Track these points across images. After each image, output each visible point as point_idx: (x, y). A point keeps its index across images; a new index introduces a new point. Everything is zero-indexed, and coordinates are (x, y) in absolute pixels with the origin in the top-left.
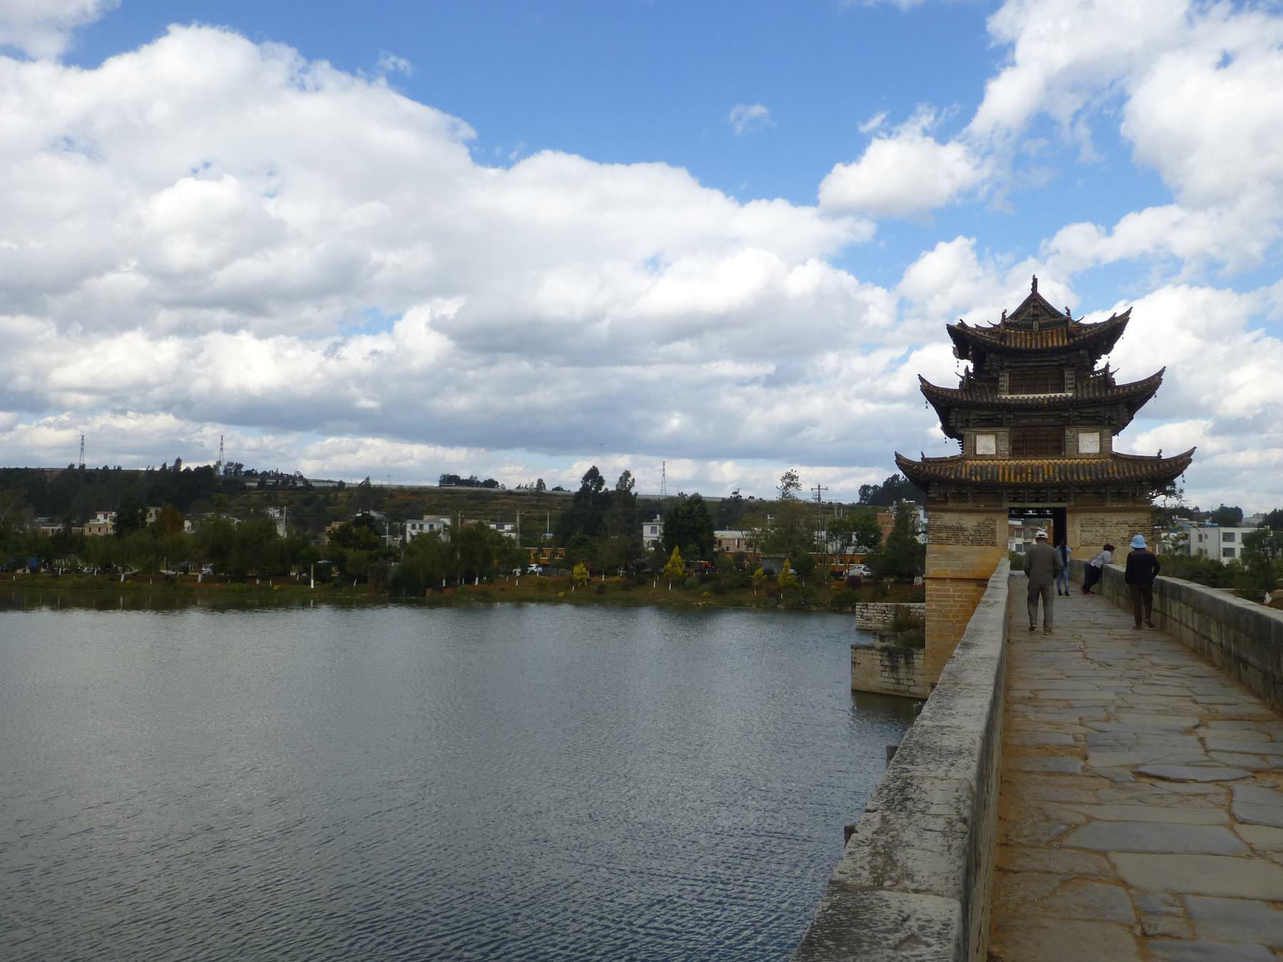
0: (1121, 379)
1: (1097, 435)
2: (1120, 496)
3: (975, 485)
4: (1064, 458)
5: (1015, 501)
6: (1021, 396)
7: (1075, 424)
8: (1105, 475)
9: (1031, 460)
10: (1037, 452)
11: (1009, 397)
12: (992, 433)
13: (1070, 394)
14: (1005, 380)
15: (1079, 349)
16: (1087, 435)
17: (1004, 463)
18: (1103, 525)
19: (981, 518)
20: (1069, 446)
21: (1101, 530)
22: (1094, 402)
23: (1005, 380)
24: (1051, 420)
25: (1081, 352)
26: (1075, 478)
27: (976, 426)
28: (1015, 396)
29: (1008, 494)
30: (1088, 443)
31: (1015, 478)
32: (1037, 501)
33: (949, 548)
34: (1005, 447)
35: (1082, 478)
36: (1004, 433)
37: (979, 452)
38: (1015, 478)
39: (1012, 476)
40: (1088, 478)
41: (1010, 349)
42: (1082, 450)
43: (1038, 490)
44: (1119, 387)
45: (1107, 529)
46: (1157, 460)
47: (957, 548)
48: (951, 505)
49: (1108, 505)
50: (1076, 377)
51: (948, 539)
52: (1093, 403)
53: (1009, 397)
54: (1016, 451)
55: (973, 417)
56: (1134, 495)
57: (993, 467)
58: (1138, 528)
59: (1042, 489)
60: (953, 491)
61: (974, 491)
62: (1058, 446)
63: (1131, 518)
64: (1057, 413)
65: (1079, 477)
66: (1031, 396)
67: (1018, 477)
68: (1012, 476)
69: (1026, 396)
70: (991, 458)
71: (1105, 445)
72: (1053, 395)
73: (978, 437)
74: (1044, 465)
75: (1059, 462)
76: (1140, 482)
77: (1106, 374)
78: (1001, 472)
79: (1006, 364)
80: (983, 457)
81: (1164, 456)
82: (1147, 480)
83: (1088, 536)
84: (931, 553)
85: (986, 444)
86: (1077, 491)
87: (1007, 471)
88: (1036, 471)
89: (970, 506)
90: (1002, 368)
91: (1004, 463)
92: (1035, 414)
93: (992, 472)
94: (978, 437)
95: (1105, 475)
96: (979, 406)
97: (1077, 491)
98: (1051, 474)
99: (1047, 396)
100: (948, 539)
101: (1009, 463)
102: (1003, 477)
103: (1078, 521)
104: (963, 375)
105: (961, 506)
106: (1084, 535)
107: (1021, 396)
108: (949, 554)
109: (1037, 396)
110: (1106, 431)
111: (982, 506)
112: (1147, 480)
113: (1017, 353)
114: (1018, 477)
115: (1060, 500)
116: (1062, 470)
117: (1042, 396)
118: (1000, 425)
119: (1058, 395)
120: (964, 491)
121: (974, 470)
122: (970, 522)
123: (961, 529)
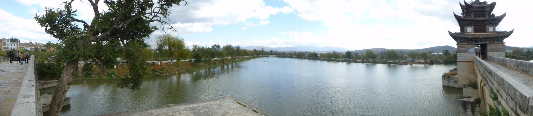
0: (496, 16)
2: (498, 40)
4: (486, 32)
5: (476, 42)
7: (488, 25)
17: (473, 34)
27: (467, 25)
30: (491, 29)
32: (481, 42)
36: (473, 27)
37: (468, 31)
43: (481, 40)
48: (461, 43)
54: (476, 30)
62: (484, 30)
71: (494, 29)
77: (493, 15)
81: (507, 31)
85: (469, 29)
96: (467, 20)
101: (474, 34)
110: (495, 26)
118: (472, 25)
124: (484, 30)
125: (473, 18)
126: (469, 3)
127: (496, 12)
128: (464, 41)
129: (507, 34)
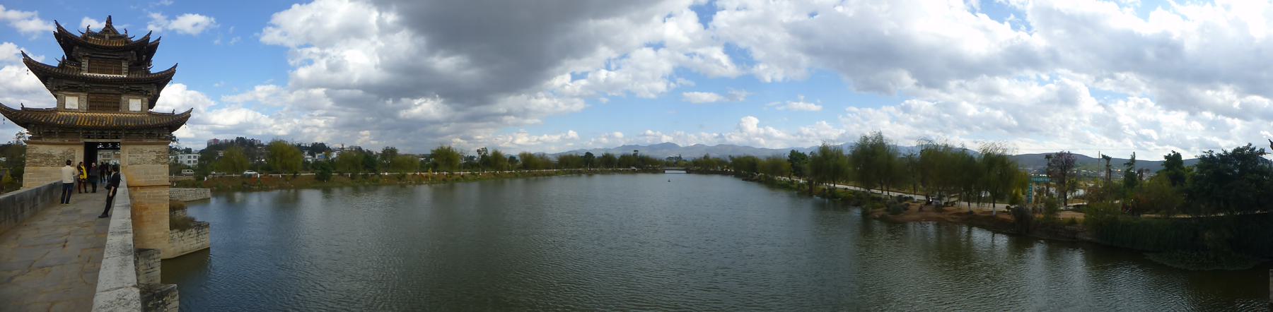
1: (140, 100)
2: (150, 135)
3: (60, 126)
5: (89, 138)
6: (95, 75)
8: (143, 123)
9: (101, 113)
10: (103, 108)
11: (88, 74)
12: (76, 96)
13: (125, 76)
14: (85, 64)
15: (130, 51)
16: (134, 100)
17: (83, 115)
18: (142, 152)
19: (65, 148)
20: (123, 106)
21: (141, 155)
22: (138, 81)
23: (85, 64)
24: (113, 91)
25: (132, 52)
26: (126, 124)
27: (65, 90)
28: (91, 74)
29: (59, 133)
30: (135, 105)
31: (88, 123)
32: (103, 138)
33: (42, 169)
34: (84, 105)
35: (129, 124)
36: (84, 96)
38: (88, 123)
39: (86, 122)
40: (133, 124)
41: (89, 44)
42: (130, 109)
44: (152, 74)
45: (144, 154)
46: (172, 115)
47: (49, 168)
49: (144, 141)
50: (129, 69)
51: (41, 162)
52: (138, 81)
53: (88, 74)
54: (91, 107)
55: (64, 84)
56: (159, 135)
57: (75, 116)
58: (161, 154)
59: (105, 130)
60: (45, 131)
61: (60, 131)
62: (116, 108)
63: (157, 148)
64: (117, 86)
65: (127, 124)
66: (102, 75)
67: (90, 123)
68: (86, 122)
69: (98, 75)
70: (75, 111)
72: (115, 76)
73: (67, 98)
74: (108, 116)
75: (117, 115)
76: (163, 127)
78: (79, 119)
79: (87, 54)
80: (70, 110)
82: (166, 126)
83: (133, 159)
84: (27, 172)
85: (72, 102)
86: (127, 132)
87: (79, 119)
88: (102, 120)
89: (57, 141)
90: (84, 56)
91: (83, 115)
92: (103, 85)
93: (73, 119)
94: (67, 98)
95: (143, 123)
96: (68, 77)
97: (127, 132)
98: (111, 121)
99: (112, 76)
100: (41, 162)
102: (80, 122)
103: (127, 150)
104: (61, 60)
105: (52, 141)
106: (131, 158)
107: (95, 75)
108: (42, 172)
109: (105, 75)
111: (67, 141)
112: (166, 126)
113: (94, 47)
114: (90, 123)
115: (117, 138)
116: (119, 119)
117: (108, 76)
119: (118, 76)
120: (53, 131)
121: (62, 118)
122: (57, 151)
123: (50, 156)
124: (116, 108)
125: (85, 74)
126: (79, 35)
127: (158, 65)
128: (49, 134)
129: (178, 120)
